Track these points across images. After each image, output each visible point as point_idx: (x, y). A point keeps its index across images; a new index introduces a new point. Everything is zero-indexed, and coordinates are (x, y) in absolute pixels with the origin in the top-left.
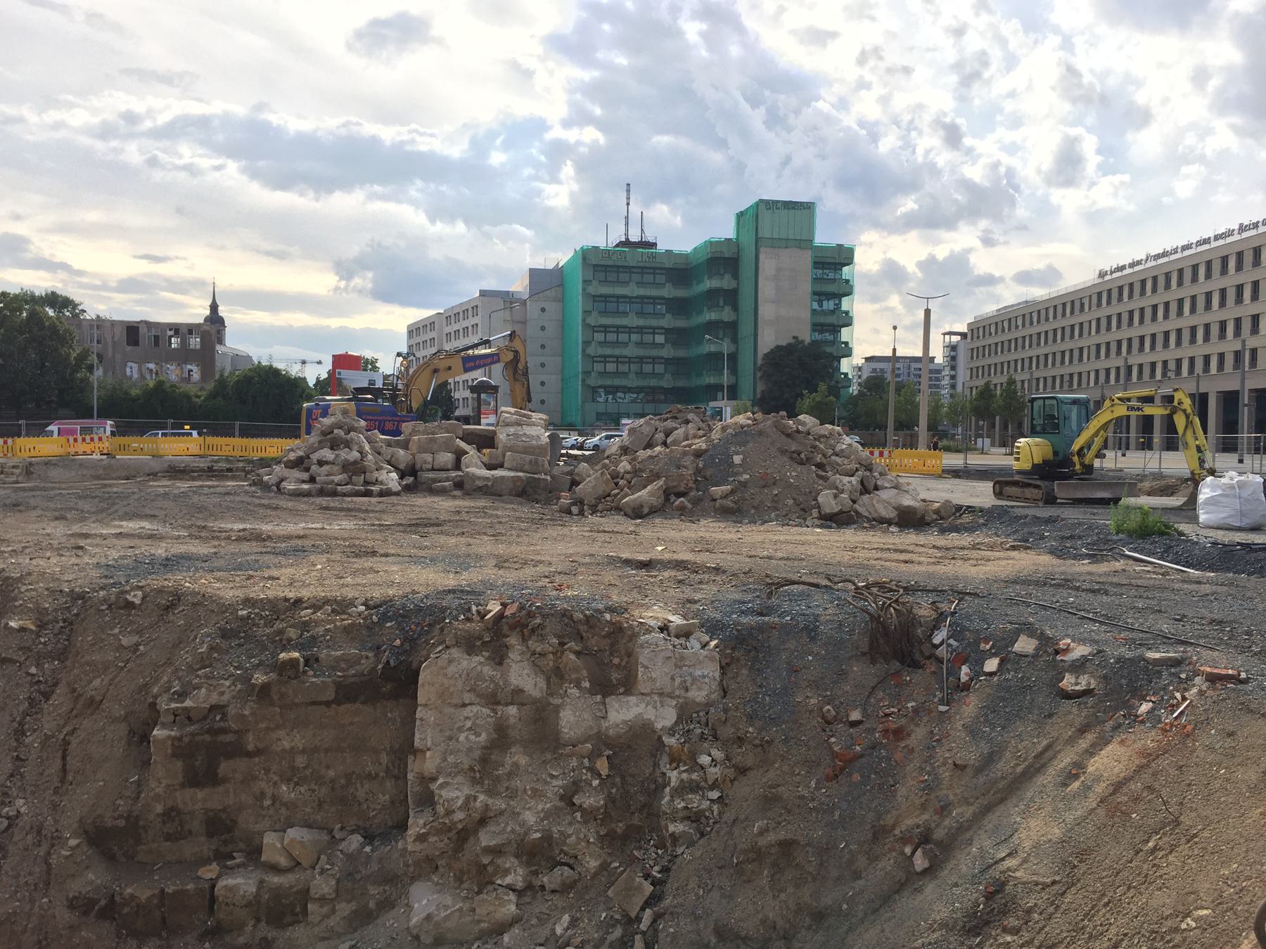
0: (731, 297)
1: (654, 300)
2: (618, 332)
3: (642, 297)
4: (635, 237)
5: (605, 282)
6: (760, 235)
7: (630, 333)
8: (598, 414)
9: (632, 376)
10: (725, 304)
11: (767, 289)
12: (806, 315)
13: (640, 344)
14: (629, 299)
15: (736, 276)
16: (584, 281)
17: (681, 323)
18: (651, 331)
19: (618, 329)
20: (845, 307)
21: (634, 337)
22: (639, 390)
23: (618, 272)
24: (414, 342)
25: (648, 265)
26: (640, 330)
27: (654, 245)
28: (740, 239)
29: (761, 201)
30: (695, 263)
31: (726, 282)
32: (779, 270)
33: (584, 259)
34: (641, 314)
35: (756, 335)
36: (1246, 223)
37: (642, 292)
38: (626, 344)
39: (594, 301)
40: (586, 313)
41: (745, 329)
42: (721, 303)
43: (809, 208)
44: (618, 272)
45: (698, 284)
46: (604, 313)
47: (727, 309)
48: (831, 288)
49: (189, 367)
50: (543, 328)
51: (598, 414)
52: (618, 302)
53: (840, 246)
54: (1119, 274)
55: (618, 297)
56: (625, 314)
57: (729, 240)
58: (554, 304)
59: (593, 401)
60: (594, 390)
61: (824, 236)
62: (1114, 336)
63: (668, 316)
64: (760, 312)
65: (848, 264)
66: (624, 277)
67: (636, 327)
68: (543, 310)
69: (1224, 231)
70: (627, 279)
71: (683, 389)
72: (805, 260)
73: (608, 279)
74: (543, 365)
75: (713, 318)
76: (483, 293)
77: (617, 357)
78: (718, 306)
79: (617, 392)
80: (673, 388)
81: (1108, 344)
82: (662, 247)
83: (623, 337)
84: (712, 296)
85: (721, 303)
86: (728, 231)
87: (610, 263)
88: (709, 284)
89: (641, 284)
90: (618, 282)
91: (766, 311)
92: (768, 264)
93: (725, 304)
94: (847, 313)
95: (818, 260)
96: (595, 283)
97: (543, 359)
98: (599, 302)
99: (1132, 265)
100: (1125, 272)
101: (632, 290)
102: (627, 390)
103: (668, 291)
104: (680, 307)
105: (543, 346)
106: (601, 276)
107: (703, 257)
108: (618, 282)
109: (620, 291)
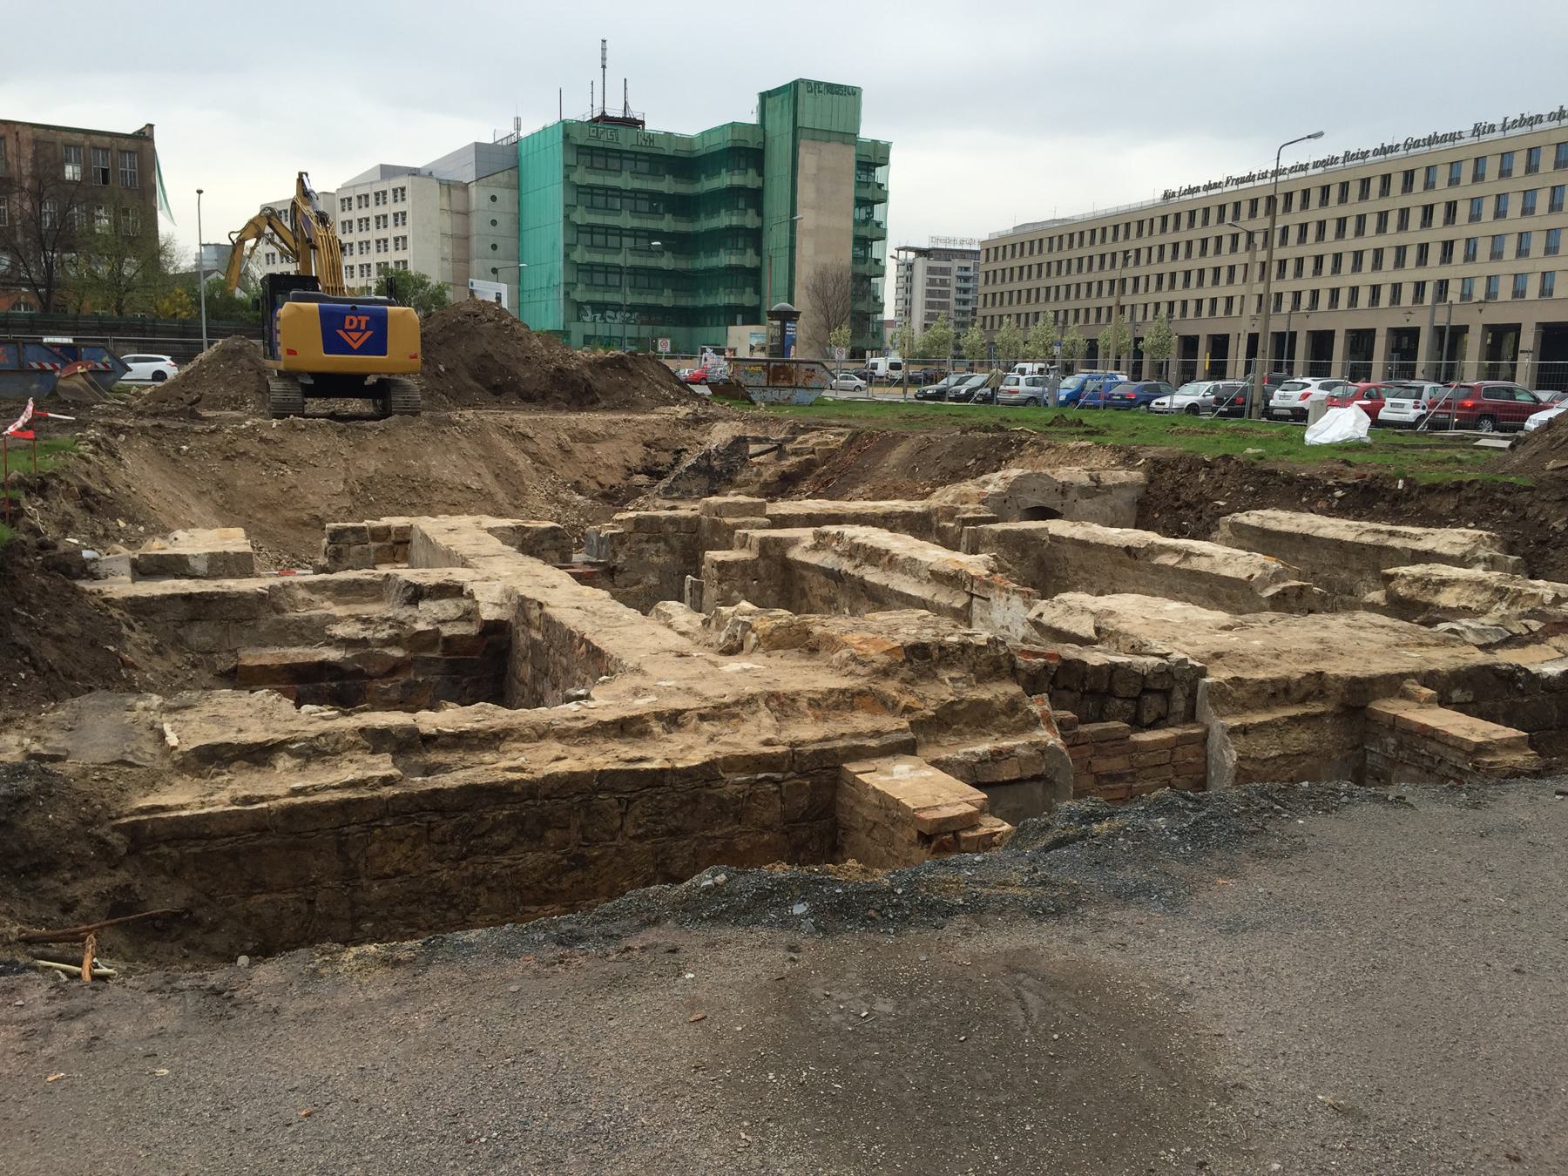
0: (755, 198)
1: (654, 196)
2: (606, 234)
4: (615, 111)
5: (591, 167)
6: (799, 124)
7: (621, 235)
8: (585, 336)
11: (806, 192)
12: (849, 224)
13: (634, 250)
14: (619, 192)
17: (683, 227)
20: (877, 217)
22: (633, 308)
25: (644, 150)
26: (635, 233)
27: (636, 123)
28: (768, 125)
29: (802, 80)
31: (749, 179)
32: (820, 169)
33: (566, 136)
34: (635, 212)
35: (792, 248)
36: (1354, 151)
37: (637, 184)
38: (618, 250)
39: (578, 193)
41: (776, 238)
42: (741, 204)
43: (854, 94)
44: (607, 156)
45: (709, 177)
46: (591, 207)
47: (751, 212)
48: (867, 194)
50: (494, 223)
51: (585, 336)
53: (875, 142)
54: (1189, 197)
55: (607, 189)
56: (617, 212)
58: (506, 191)
60: (579, 306)
61: (867, 132)
62: (1086, 251)
63: (668, 217)
65: (881, 165)
67: (630, 230)
68: (494, 198)
69: (1326, 158)
71: (686, 309)
72: (849, 157)
73: (596, 165)
75: (734, 223)
78: (737, 208)
80: (673, 307)
81: (1069, 261)
82: (651, 126)
83: (613, 241)
84: (731, 197)
85: (741, 204)
86: (749, 115)
87: (601, 145)
88: (725, 180)
89: (636, 174)
90: (606, 169)
91: (806, 218)
92: (808, 160)
94: (878, 224)
95: (864, 159)
96: (581, 169)
97: (496, 264)
98: (581, 193)
99: (1208, 187)
100: (1197, 195)
101: (625, 181)
102: (617, 307)
103: (667, 185)
104: (684, 206)
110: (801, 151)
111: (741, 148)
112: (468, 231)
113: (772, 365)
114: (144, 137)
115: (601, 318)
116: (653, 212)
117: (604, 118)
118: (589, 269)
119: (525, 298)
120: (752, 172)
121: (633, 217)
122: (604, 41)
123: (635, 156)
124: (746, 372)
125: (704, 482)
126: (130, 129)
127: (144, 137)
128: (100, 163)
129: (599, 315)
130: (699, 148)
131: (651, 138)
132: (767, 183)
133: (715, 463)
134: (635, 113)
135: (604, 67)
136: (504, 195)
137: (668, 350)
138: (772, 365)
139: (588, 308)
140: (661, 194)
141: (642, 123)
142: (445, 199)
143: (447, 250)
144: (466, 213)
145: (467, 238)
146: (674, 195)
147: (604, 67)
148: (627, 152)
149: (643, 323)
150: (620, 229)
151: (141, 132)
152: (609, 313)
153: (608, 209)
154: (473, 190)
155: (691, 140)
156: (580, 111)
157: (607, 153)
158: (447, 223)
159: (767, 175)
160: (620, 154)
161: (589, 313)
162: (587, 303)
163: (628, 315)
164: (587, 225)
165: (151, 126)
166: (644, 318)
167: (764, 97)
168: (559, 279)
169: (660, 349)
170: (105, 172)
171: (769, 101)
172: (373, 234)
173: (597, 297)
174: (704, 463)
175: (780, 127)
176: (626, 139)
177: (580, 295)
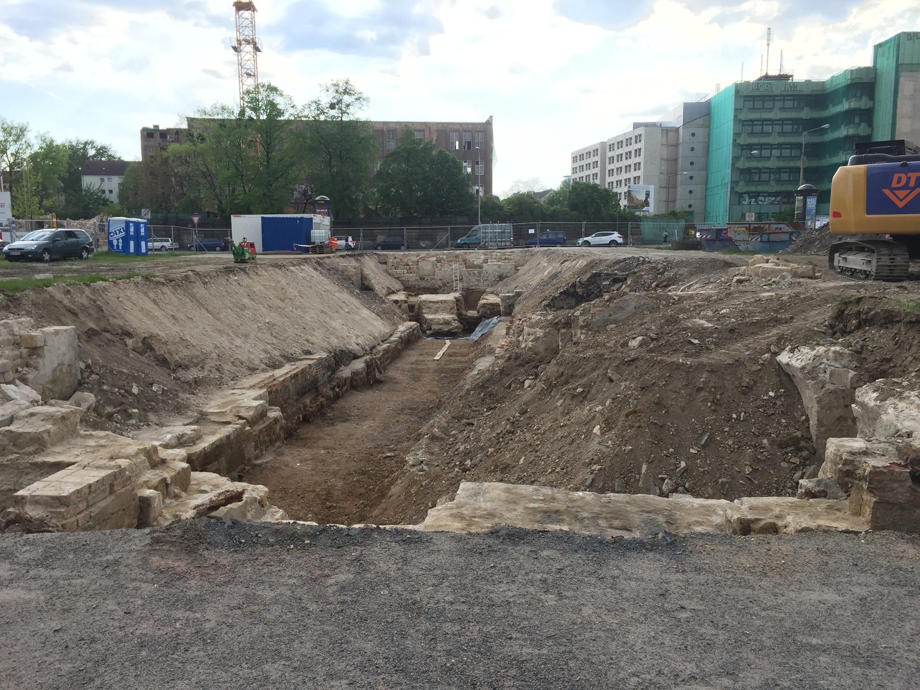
3: (782, 120)
7: (771, 149)
9: (773, 183)
10: (861, 121)
11: (905, 107)
13: (780, 158)
15: (872, 97)
16: (736, 110)
18: (769, 147)
19: (761, 147)
21: (776, 152)
22: (776, 194)
23: (764, 101)
24: (577, 165)
25: (790, 93)
26: (780, 146)
28: (878, 66)
29: (904, 33)
30: (830, 90)
37: (784, 115)
38: (768, 158)
40: (737, 135)
42: (857, 120)
45: (834, 105)
46: (752, 134)
49: (477, 188)
50: (693, 149)
52: (762, 125)
55: (763, 120)
56: (769, 134)
57: (868, 68)
59: (739, 203)
60: (740, 195)
64: (898, 126)
66: (769, 104)
68: (693, 135)
70: (771, 106)
73: (756, 106)
74: (691, 178)
76: (636, 126)
77: (760, 169)
78: (854, 124)
79: (759, 196)
83: (766, 153)
84: (849, 116)
85: (857, 120)
86: (866, 61)
87: (759, 94)
89: (783, 109)
90: (763, 108)
93: (861, 121)
103: (806, 114)
105: (692, 163)
106: (750, 104)
107: (843, 82)
108: (763, 108)
109: (765, 115)
110: (901, 80)
111: (857, 84)
112: (677, 155)
113: (752, 226)
114: (489, 123)
115: (756, 202)
116: (793, 133)
117: (767, 77)
118: (748, 171)
119: (709, 193)
120: (865, 98)
121: (780, 136)
122: (769, 29)
123: (784, 97)
124: (735, 232)
125: (573, 301)
126: (483, 120)
127: (489, 123)
128: (467, 137)
129: (753, 200)
130: (829, 88)
131: (795, 85)
132: (876, 105)
133: (578, 290)
134: (786, 71)
135: (768, 45)
136: (700, 132)
137: (753, 219)
138: (752, 226)
139: (746, 196)
140: (801, 119)
141: (792, 76)
142: (664, 139)
143: (664, 168)
144: (677, 145)
145: (676, 160)
146: (810, 119)
147: (768, 45)
148: (777, 96)
149: (784, 203)
150: (771, 145)
151: (488, 121)
152: (760, 198)
153: (762, 134)
154: (681, 131)
155: (823, 83)
156: (752, 76)
157: (764, 98)
158: (664, 152)
159: (877, 98)
160: (773, 98)
161: (747, 199)
162: (746, 193)
163: (774, 198)
164: (748, 145)
165: (491, 117)
166: (785, 200)
167: (878, 47)
168: (728, 179)
169: (747, 219)
170: (469, 143)
171: (880, 50)
172: (623, 163)
173: (753, 189)
174: (572, 290)
175: (888, 65)
176: (778, 88)
177: (739, 189)
